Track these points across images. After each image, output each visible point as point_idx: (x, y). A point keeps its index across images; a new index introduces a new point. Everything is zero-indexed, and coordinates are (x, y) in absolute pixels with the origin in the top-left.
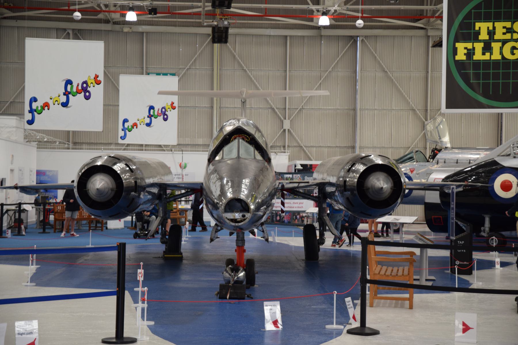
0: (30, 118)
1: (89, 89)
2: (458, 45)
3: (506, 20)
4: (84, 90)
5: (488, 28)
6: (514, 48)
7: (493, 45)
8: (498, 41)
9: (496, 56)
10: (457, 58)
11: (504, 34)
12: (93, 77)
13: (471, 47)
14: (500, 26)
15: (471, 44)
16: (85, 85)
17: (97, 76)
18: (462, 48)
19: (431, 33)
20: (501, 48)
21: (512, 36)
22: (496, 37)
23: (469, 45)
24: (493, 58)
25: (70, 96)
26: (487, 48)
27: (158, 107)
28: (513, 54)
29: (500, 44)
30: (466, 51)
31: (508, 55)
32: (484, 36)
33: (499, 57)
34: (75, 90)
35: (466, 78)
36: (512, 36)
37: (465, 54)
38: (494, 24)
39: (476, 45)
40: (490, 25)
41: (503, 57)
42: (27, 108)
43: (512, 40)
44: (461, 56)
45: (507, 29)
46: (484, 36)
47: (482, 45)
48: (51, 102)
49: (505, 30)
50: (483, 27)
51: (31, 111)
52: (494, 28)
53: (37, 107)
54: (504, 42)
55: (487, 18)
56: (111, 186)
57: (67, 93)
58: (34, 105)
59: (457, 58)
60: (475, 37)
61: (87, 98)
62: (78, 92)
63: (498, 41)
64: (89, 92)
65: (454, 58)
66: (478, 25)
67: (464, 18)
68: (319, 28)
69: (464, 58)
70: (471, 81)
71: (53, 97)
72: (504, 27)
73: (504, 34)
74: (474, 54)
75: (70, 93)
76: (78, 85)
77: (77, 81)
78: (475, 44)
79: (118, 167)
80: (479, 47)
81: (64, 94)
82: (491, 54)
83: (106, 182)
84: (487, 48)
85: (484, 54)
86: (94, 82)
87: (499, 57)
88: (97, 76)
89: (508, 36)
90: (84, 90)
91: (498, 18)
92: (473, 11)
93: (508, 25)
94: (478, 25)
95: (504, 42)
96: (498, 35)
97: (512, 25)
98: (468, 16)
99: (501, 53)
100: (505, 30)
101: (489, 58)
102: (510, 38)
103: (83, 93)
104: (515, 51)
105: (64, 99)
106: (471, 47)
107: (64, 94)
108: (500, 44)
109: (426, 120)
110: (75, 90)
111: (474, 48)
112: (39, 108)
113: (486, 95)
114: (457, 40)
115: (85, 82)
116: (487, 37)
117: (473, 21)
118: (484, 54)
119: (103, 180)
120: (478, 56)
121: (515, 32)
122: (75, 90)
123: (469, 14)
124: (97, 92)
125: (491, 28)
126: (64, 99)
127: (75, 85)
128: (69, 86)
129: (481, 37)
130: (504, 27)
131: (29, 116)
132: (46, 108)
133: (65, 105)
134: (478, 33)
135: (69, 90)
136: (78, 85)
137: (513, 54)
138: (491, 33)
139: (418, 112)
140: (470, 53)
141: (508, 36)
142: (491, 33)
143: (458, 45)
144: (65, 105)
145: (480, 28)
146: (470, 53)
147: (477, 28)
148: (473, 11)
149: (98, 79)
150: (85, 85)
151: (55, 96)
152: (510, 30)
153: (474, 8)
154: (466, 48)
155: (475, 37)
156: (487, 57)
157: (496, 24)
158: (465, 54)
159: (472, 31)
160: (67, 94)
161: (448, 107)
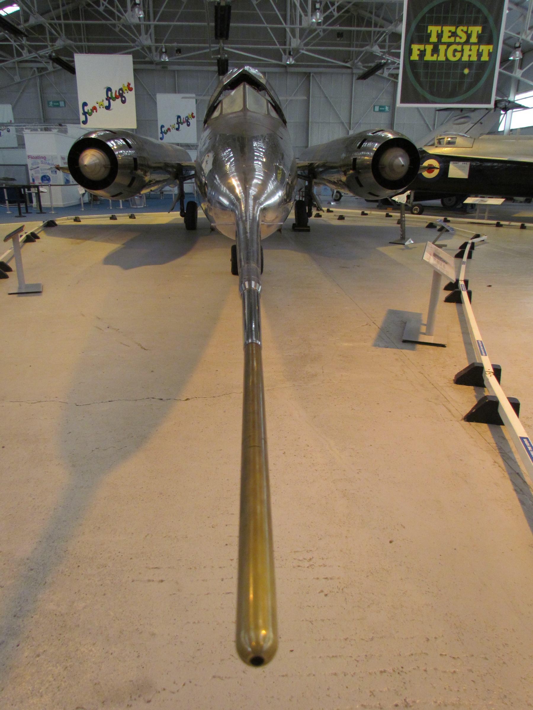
0: (84, 119)
1: (124, 95)
3: (451, 24)
4: (121, 95)
6: (455, 51)
8: (444, 43)
9: (442, 58)
10: (412, 58)
11: (449, 37)
12: (126, 85)
14: (447, 30)
16: (121, 92)
17: (129, 84)
18: (416, 48)
19: (355, 71)
20: (446, 50)
21: (455, 40)
22: (443, 40)
23: (422, 47)
25: (111, 101)
26: (436, 50)
27: (183, 116)
28: (454, 56)
29: (445, 47)
30: (418, 52)
34: (113, 96)
35: (416, 75)
36: (455, 40)
37: (418, 55)
38: (442, 28)
40: (439, 28)
42: (81, 111)
43: (455, 43)
44: (415, 57)
46: (434, 39)
49: (450, 34)
50: (433, 30)
51: (85, 113)
52: (442, 32)
53: (88, 110)
54: (449, 45)
55: (437, 23)
59: (412, 58)
61: (124, 102)
62: (117, 97)
63: (444, 43)
64: (124, 97)
65: (409, 58)
66: (430, 28)
68: (286, 66)
70: (421, 79)
72: (450, 31)
73: (449, 37)
74: (425, 55)
75: (110, 98)
77: (115, 89)
78: (426, 46)
79: (112, 144)
80: (429, 48)
82: (438, 55)
83: (98, 159)
84: (436, 50)
85: (432, 55)
88: (129, 84)
89: (452, 40)
90: (121, 95)
92: (427, 15)
93: (453, 29)
94: (430, 28)
95: (449, 45)
96: (445, 39)
98: (423, 19)
99: (446, 55)
101: (436, 60)
102: (453, 41)
103: (120, 99)
104: (456, 54)
105: (106, 103)
107: (107, 99)
108: (445, 47)
109: (350, 129)
110: (114, 96)
111: (425, 50)
112: (90, 111)
113: (432, 93)
114: (412, 42)
115: (121, 89)
117: (426, 25)
118: (432, 55)
119: (94, 155)
120: (428, 57)
121: (457, 36)
122: (113, 96)
123: (423, 18)
124: (130, 96)
125: (440, 32)
126: (106, 103)
128: (109, 93)
130: (450, 31)
131: (82, 118)
132: (95, 111)
134: (429, 36)
135: (110, 96)
137: (454, 56)
138: (440, 36)
139: (345, 124)
140: (422, 54)
141: (452, 40)
142: (440, 36)
145: (431, 31)
146: (422, 54)
147: (429, 32)
148: (427, 15)
149: (130, 86)
150: (121, 92)
151: (100, 101)
154: (419, 50)
156: (434, 58)
158: (418, 55)
159: (425, 34)
161: (402, 101)
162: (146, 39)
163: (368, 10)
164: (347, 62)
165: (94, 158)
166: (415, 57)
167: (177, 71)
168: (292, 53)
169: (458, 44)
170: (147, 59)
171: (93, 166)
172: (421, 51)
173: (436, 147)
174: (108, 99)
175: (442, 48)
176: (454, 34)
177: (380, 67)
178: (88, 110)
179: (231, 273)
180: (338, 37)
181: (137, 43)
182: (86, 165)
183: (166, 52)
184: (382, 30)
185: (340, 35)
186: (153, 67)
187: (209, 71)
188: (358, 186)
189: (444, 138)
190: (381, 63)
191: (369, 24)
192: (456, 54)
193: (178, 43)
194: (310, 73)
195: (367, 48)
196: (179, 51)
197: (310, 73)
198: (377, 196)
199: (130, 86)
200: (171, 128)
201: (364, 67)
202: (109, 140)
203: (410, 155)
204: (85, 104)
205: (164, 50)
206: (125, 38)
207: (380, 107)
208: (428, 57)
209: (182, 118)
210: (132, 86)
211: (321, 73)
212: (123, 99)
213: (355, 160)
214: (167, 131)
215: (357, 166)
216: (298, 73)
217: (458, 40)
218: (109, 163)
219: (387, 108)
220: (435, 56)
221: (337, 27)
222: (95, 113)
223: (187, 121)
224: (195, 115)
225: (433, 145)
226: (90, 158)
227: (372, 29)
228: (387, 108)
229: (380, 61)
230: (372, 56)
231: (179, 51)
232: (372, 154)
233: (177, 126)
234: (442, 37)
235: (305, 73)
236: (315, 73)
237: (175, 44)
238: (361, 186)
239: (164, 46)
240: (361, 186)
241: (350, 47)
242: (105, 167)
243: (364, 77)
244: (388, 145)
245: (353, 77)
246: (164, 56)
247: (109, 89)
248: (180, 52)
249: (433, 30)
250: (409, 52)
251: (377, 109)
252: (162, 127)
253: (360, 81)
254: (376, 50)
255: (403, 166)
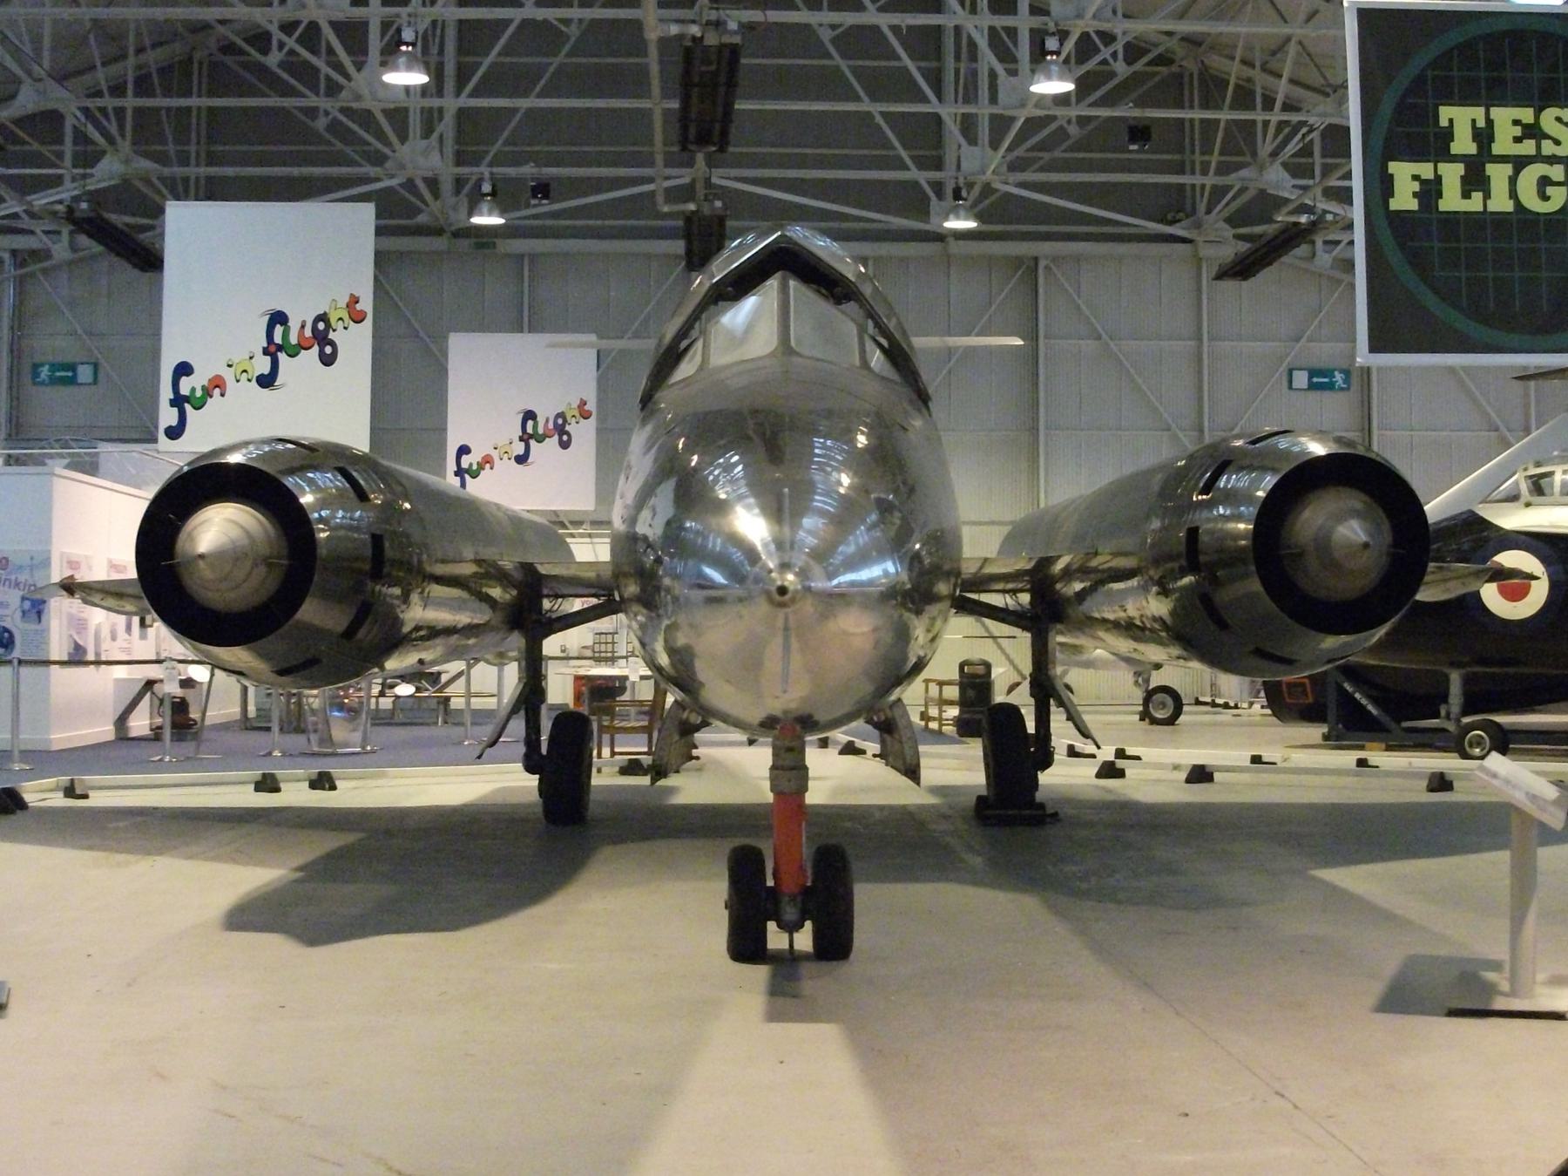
0: (174, 422)
1: (332, 335)
2: (1394, 167)
4: (322, 339)
5: (1474, 121)
6: (1544, 182)
7: (1492, 170)
9: (1500, 202)
10: (1395, 205)
11: (1517, 140)
12: (343, 301)
13: (1431, 176)
14: (1504, 116)
15: (1430, 166)
16: (321, 326)
17: (355, 300)
18: (1405, 175)
20: (1513, 181)
21: (1539, 147)
22: (1497, 149)
23: (1426, 170)
24: (1493, 206)
25: (282, 356)
26: (1475, 180)
27: (545, 414)
28: (1545, 197)
29: (1508, 169)
30: (1416, 186)
31: (1532, 202)
32: (1463, 144)
33: (1509, 206)
36: (1539, 147)
37: (1415, 195)
39: (1444, 168)
40: (1478, 113)
41: (1518, 204)
42: (166, 393)
43: (1538, 158)
44: (1404, 199)
45: (1526, 127)
46: (1463, 144)
47: (1459, 169)
48: (228, 376)
49: (1518, 131)
50: (1460, 119)
51: (178, 401)
52: (1490, 122)
53: (193, 390)
54: (1520, 163)
55: (1466, 98)
56: (265, 550)
57: (273, 348)
58: (185, 386)
59: (1395, 205)
60: (1436, 146)
61: (328, 360)
62: (302, 346)
64: (332, 344)
67: (1408, 92)
68: (940, 237)
69: (1413, 205)
71: (236, 361)
72: (1516, 122)
73: (1517, 140)
74: (1440, 195)
76: (303, 327)
77: (301, 316)
80: (1452, 174)
81: (266, 352)
82: (1487, 196)
84: (1475, 180)
85: (1466, 195)
86: (346, 316)
87: (1509, 206)
88: (355, 300)
89: (1528, 148)
90: (322, 339)
91: (1493, 94)
93: (1527, 115)
94: (1446, 113)
95: (1520, 163)
96: (1503, 144)
97: (1537, 117)
99: (1513, 194)
100: (1518, 131)
102: (1533, 152)
103: (316, 348)
104: (1550, 190)
105: (263, 365)
106: (1431, 176)
107: (266, 352)
108: (1508, 169)
110: (294, 340)
111: (1438, 179)
112: (199, 394)
115: (323, 317)
116: (1472, 149)
118: (1466, 195)
120: (1452, 200)
123: (1419, 82)
124: (355, 343)
125: (1481, 123)
127: (294, 325)
128: (279, 330)
129: (1456, 148)
130: (1516, 122)
133: (266, 381)
134: (1448, 134)
135: (278, 339)
136: (303, 327)
137: (1545, 197)
138: (1484, 136)
140: (1430, 191)
141: (1528, 148)
142: (1484, 136)
143: (1394, 167)
144: (266, 381)
145: (1451, 121)
146: (1430, 191)
147: (1444, 123)
148: (1429, 73)
149: (358, 307)
152: (1532, 131)
153: (1434, 64)
154: (1416, 178)
155: (1436, 146)
156: (1475, 204)
157: (1496, 112)
158: (1415, 195)
160: (272, 351)
161: (1374, 349)
162: (426, 152)
163: (1238, 54)
164: (1172, 223)
165: (235, 533)
166: (1404, 199)
167: (534, 257)
168: (964, 194)
169: (1552, 160)
170: (422, 219)
171: (227, 557)
172: (1424, 182)
173: (1528, 505)
174: (272, 350)
175: (1498, 174)
176: (1532, 131)
177: (1292, 237)
178: (193, 390)
179: (727, 956)
180: (1133, 140)
181: (388, 165)
182: (202, 556)
183: (493, 194)
184: (1294, 118)
185: (1139, 132)
186: (440, 243)
187: (648, 257)
188: (1213, 627)
189: (1551, 474)
190: (1296, 224)
191: (1244, 98)
192: (1550, 190)
193: (538, 165)
194: (1036, 259)
195: (1244, 173)
196: (542, 190)
197: (1036, 259)
198: (1288, 662)
199: (358, 307)
200: (495, 455)
201: (1238, 237)
202: (292, 471)
203: (1391, 513)
204: (184, 369)
205: (487, 188)
206: (348, 150)
207: (1313, 373)
208: (1452, 200)
209: (541, 420)
210: (366, 305)
211: (1078, 259)
212: (328, 350)
213: (1193, 533)
214: (481, 467)
215: (1202, 558)
216: (990, 260)
217: (1548, 148)
218: (285, 552)
219: (1339, 377)
220: (1477, 196)
221: (1127, 111)
222: (215, 401)
223: (561, 430)
224: (591, 406)
225: (1513, 498)
226: (217, 528)
227: (1258, 116)
228: (1339, 377)
229: (1293, 219)
230: (1266, 204)
231: (542, 190)
232: (1253, 511)
233: (519, 449)
234: (1491, 139)
235: (1018, 262)
236: (1055, 259)
237: (528, 170)
238: (1222, 625)
239: (487, 175)
240: (1222, 625)
241: (1182, 172)
242: (268, 562)
243: (1242, 269)
244: (1306, 479)
245: (1199, 268)
246: (485, 207)
247: (278, 318)
248: (546, 196)
249: (1460, 119)
250: (1381, 186)
251: (1301, 379)
252: (464, 450)
253: (1229, 285)
254: (1276, 179)
255: (1366, 546)
